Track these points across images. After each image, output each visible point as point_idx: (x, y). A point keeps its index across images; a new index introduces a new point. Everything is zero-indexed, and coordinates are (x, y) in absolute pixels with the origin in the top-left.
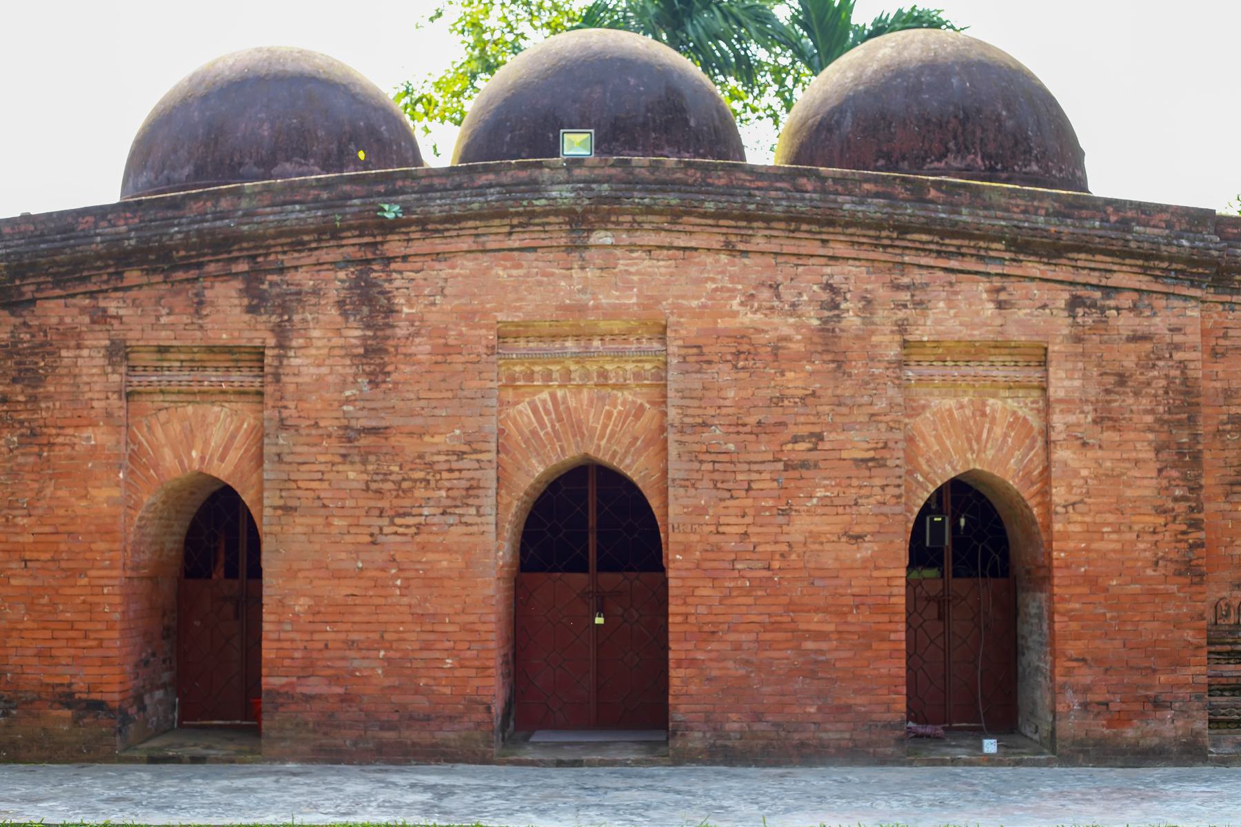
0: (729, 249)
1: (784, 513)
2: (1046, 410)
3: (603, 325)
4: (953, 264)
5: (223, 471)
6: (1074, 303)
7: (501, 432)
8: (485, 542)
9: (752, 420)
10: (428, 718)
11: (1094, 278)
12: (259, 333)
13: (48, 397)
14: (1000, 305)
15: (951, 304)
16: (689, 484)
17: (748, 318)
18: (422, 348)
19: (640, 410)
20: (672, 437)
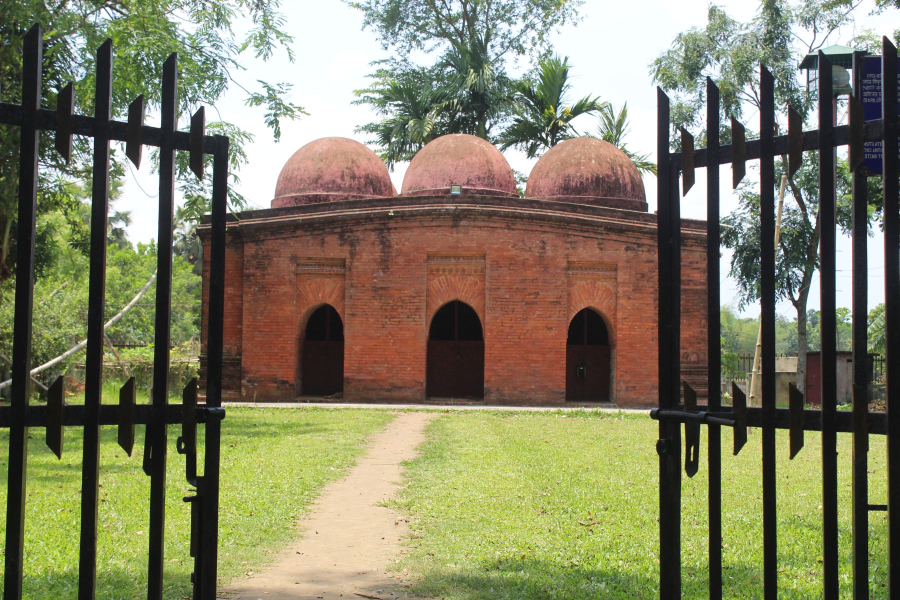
0: (509, 228)
1: (525, 319)
2: (616, 286)
3: (464, 253)
4: (586, 234)
5: (330, 301)
6: (627, 249)
7: (428, 290)
8: (420, 328)
9: (515, 287)
10: (401, 388)
11: (634, 241)
12: (344, 252)
13: (268, 274)
14: (601, 249)
15: (584, 248)
16: (493, 309)
17: (514, 252)
18: (401, 260)
19: (476, 283)
20: (487, 292)
